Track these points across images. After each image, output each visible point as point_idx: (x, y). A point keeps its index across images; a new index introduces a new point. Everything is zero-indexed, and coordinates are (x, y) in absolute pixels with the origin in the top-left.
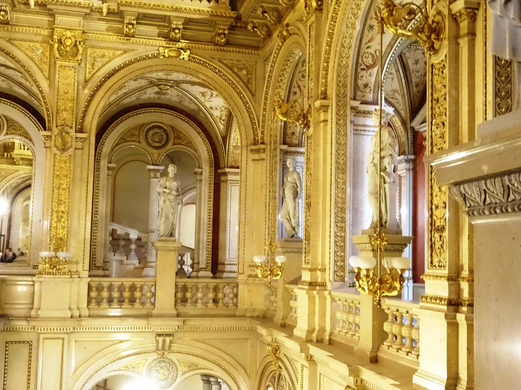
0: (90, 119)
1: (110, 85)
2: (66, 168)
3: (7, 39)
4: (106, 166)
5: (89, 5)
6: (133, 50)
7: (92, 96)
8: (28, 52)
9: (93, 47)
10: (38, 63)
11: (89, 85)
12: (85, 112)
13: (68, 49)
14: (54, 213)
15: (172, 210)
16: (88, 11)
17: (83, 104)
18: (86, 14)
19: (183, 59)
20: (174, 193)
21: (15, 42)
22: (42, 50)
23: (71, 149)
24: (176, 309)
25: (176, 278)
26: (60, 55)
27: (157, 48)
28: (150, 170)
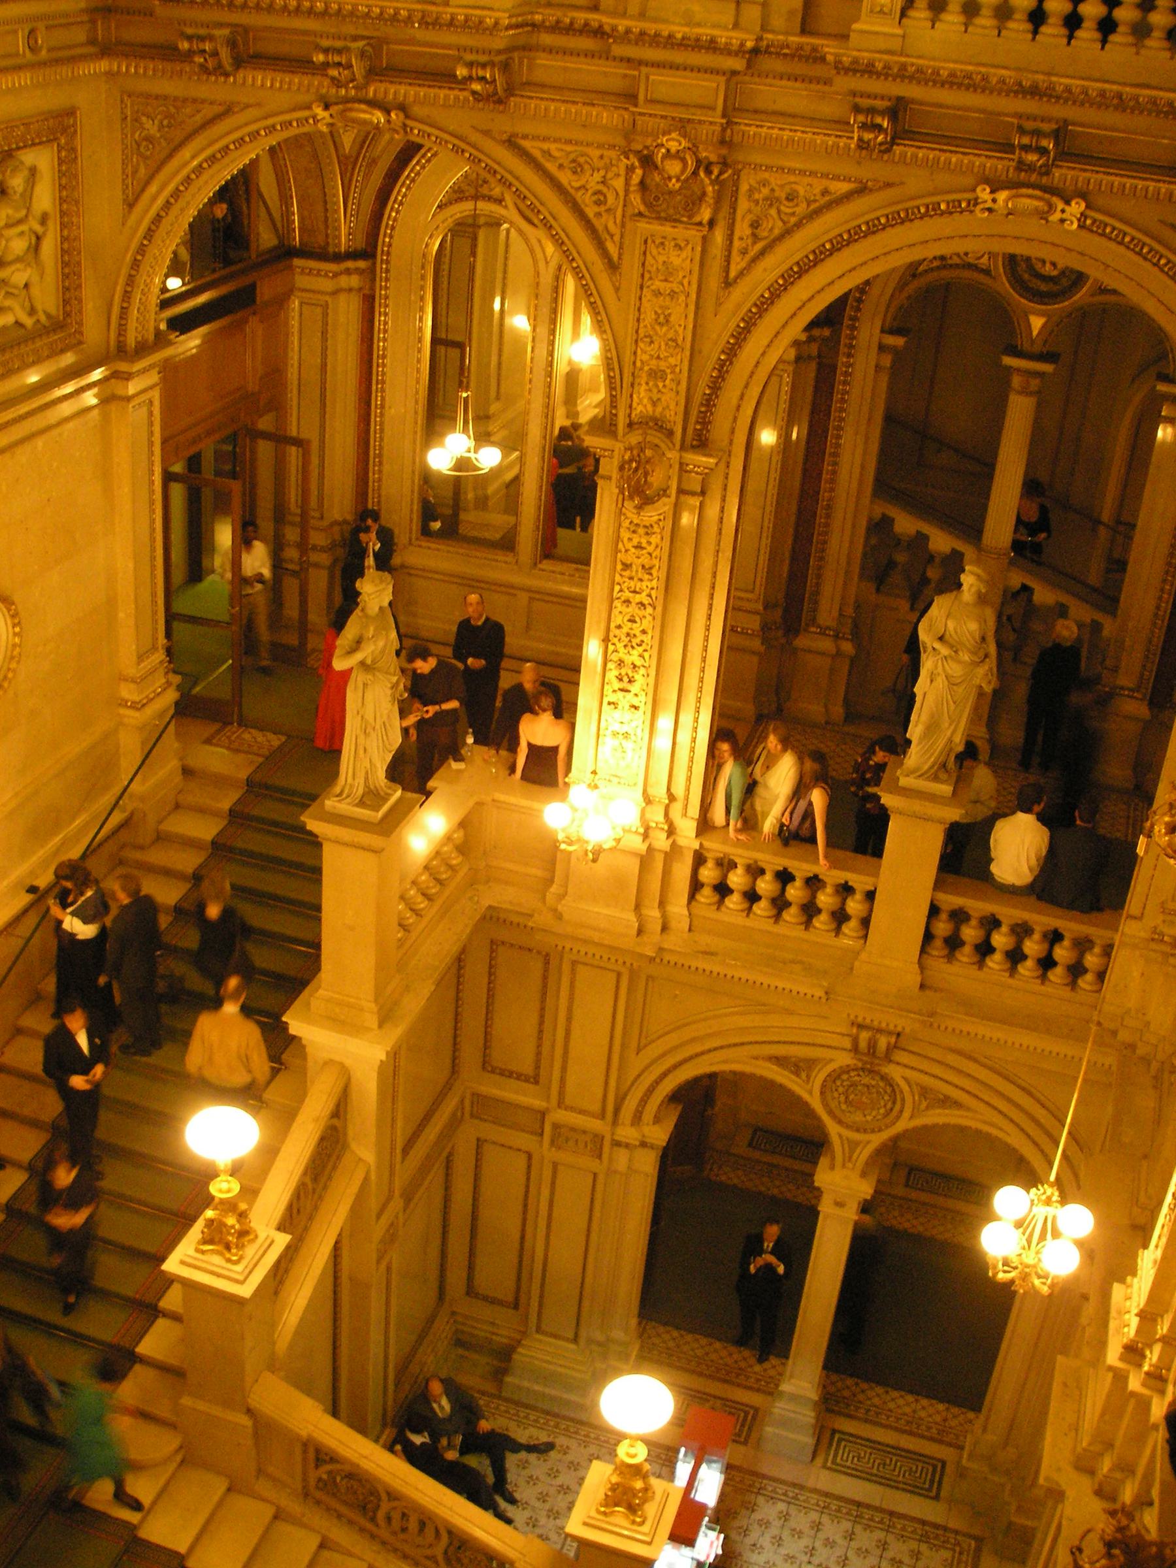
0: (735, 402)
1: (805, 297)
2: (650, 549)
3: (505, 137)
4: (876, 339)
5: (742, 45)
6: (889, 185)
7: (741, 336)
8: (565, 178)
9: (757, 167)
10: (590, 212)
11: (737, 293)
12: (716, 386)
13: (674, 185)
14: (610, 665)
15: (952, 706)
16: (738, 64)
17: (712, 353)
18: (734, 73)
19: (1062, 221)
20: (966, 657)
21: (526, 144)
22: (602, 173)
23: (665, 500)
24: (922, 967)
25: (938, 885)
26: (649, 205)
27: (969, 181)
28: (1009, 369)
